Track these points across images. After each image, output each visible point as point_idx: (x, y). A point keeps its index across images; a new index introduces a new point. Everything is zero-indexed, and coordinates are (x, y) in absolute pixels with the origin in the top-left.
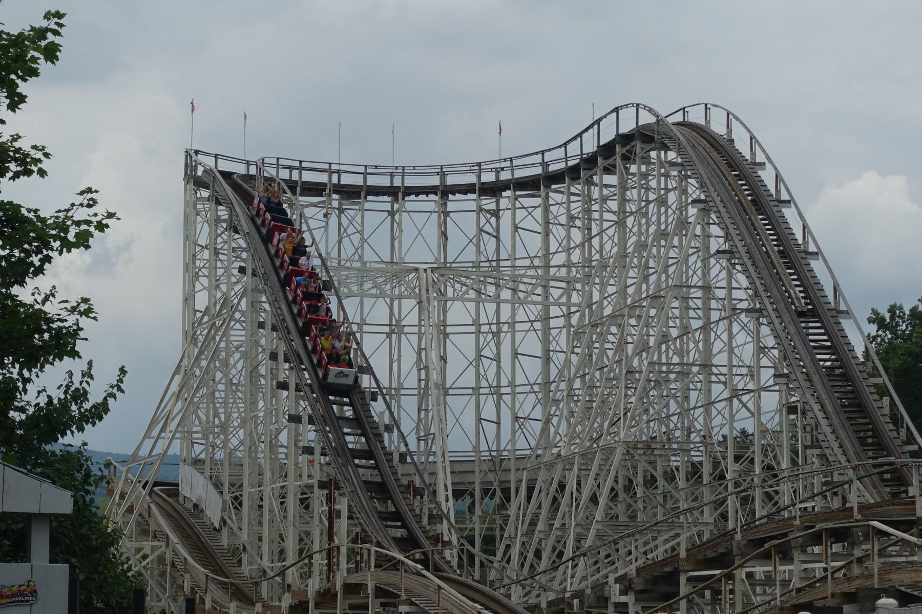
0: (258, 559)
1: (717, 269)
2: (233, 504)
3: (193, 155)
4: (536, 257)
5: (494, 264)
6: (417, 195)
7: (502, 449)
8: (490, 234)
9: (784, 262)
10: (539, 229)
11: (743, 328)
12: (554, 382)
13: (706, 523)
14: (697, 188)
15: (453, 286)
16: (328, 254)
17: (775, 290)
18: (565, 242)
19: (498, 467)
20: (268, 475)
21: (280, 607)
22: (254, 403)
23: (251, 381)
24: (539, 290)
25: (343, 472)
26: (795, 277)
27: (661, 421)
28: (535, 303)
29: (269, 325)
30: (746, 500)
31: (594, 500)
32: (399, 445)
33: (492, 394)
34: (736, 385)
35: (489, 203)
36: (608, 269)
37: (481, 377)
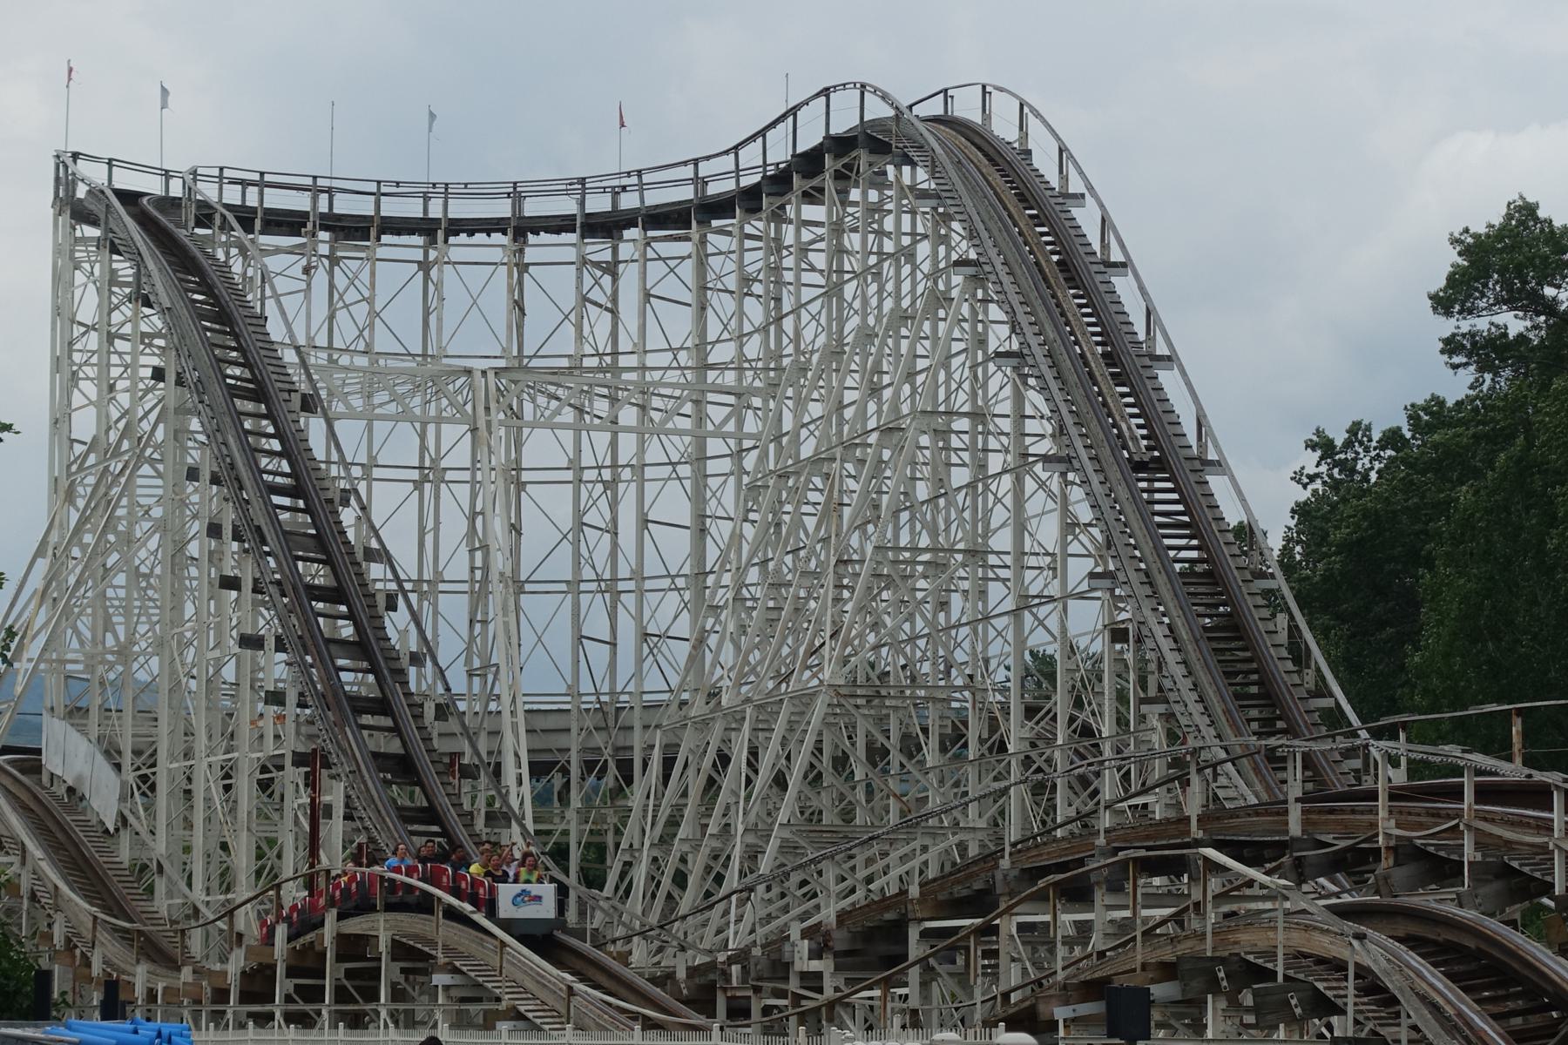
0: (183, 886)
1: (998, 380)
2: (139, 788)
3: (69, 161)
4: (682, 348)
5: (608, 359)
6: (471, 233)
7: (618, 690)
8: (600, 306)
9: (1112, 374)
10: (688, 297)
11: (1040, 487)
12: (711, 572)
13: (974, 829)
14: (963, 238)
15: (533, 400)
16: (310, 338)
17: (1094, 424)
18: (733, 322)
19: (611, 723)
20: (201, 741)
21: (225, 973)
22: (178, 608)
23: (173, 572)
24: (688, 408)
25: (336, 738)
26: (1131, 400)
27: (896, 646)
28: (681, 433)
30: (1041, 789)
31: (780, 782)
32: (435, 683)
33: (603, 592)
34: (1027, 588)
35: (599, 250)
36: (810, 374)
37: (583, 561)
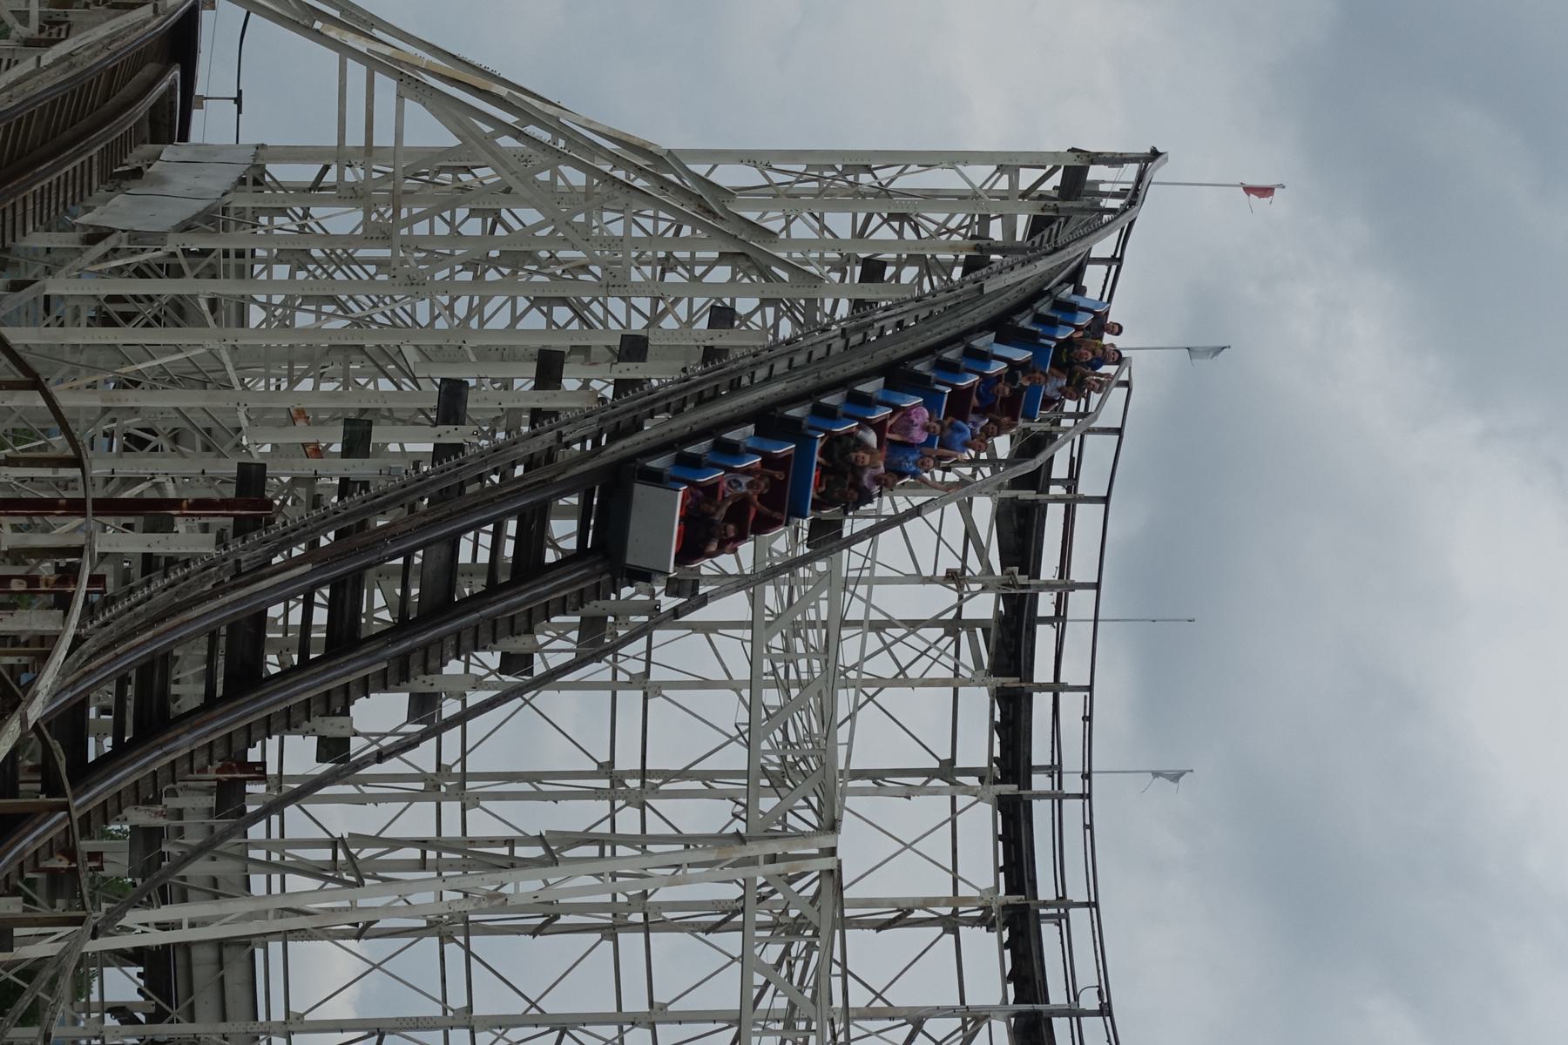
29: (722, 339)
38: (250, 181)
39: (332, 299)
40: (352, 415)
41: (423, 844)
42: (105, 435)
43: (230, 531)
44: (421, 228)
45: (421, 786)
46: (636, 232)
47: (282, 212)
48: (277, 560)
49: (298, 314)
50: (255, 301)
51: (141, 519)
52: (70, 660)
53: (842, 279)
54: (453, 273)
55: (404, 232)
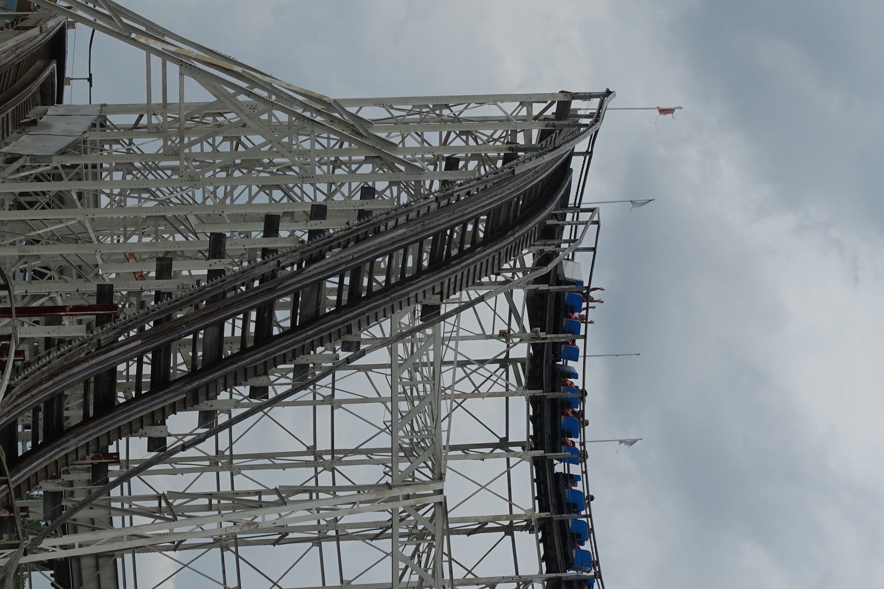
29: (368, 205)
38: (98, 125)
39: (147, 190)
40: (161, 255)
41: (209, 495)
42: (21, 271)
43: (94, 324)
44: (196, 149)
45: (207, 463)
46: (318, 147)
47: (117, 142)
48: (121, 338)
49: (128, 199)
50: (103, 193)
51: (44, 318)
52: (6, 399)
53: (435, 169)
54: (215, 174)
55: (187, 151)
